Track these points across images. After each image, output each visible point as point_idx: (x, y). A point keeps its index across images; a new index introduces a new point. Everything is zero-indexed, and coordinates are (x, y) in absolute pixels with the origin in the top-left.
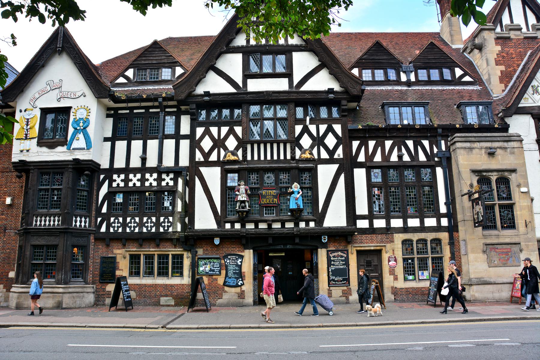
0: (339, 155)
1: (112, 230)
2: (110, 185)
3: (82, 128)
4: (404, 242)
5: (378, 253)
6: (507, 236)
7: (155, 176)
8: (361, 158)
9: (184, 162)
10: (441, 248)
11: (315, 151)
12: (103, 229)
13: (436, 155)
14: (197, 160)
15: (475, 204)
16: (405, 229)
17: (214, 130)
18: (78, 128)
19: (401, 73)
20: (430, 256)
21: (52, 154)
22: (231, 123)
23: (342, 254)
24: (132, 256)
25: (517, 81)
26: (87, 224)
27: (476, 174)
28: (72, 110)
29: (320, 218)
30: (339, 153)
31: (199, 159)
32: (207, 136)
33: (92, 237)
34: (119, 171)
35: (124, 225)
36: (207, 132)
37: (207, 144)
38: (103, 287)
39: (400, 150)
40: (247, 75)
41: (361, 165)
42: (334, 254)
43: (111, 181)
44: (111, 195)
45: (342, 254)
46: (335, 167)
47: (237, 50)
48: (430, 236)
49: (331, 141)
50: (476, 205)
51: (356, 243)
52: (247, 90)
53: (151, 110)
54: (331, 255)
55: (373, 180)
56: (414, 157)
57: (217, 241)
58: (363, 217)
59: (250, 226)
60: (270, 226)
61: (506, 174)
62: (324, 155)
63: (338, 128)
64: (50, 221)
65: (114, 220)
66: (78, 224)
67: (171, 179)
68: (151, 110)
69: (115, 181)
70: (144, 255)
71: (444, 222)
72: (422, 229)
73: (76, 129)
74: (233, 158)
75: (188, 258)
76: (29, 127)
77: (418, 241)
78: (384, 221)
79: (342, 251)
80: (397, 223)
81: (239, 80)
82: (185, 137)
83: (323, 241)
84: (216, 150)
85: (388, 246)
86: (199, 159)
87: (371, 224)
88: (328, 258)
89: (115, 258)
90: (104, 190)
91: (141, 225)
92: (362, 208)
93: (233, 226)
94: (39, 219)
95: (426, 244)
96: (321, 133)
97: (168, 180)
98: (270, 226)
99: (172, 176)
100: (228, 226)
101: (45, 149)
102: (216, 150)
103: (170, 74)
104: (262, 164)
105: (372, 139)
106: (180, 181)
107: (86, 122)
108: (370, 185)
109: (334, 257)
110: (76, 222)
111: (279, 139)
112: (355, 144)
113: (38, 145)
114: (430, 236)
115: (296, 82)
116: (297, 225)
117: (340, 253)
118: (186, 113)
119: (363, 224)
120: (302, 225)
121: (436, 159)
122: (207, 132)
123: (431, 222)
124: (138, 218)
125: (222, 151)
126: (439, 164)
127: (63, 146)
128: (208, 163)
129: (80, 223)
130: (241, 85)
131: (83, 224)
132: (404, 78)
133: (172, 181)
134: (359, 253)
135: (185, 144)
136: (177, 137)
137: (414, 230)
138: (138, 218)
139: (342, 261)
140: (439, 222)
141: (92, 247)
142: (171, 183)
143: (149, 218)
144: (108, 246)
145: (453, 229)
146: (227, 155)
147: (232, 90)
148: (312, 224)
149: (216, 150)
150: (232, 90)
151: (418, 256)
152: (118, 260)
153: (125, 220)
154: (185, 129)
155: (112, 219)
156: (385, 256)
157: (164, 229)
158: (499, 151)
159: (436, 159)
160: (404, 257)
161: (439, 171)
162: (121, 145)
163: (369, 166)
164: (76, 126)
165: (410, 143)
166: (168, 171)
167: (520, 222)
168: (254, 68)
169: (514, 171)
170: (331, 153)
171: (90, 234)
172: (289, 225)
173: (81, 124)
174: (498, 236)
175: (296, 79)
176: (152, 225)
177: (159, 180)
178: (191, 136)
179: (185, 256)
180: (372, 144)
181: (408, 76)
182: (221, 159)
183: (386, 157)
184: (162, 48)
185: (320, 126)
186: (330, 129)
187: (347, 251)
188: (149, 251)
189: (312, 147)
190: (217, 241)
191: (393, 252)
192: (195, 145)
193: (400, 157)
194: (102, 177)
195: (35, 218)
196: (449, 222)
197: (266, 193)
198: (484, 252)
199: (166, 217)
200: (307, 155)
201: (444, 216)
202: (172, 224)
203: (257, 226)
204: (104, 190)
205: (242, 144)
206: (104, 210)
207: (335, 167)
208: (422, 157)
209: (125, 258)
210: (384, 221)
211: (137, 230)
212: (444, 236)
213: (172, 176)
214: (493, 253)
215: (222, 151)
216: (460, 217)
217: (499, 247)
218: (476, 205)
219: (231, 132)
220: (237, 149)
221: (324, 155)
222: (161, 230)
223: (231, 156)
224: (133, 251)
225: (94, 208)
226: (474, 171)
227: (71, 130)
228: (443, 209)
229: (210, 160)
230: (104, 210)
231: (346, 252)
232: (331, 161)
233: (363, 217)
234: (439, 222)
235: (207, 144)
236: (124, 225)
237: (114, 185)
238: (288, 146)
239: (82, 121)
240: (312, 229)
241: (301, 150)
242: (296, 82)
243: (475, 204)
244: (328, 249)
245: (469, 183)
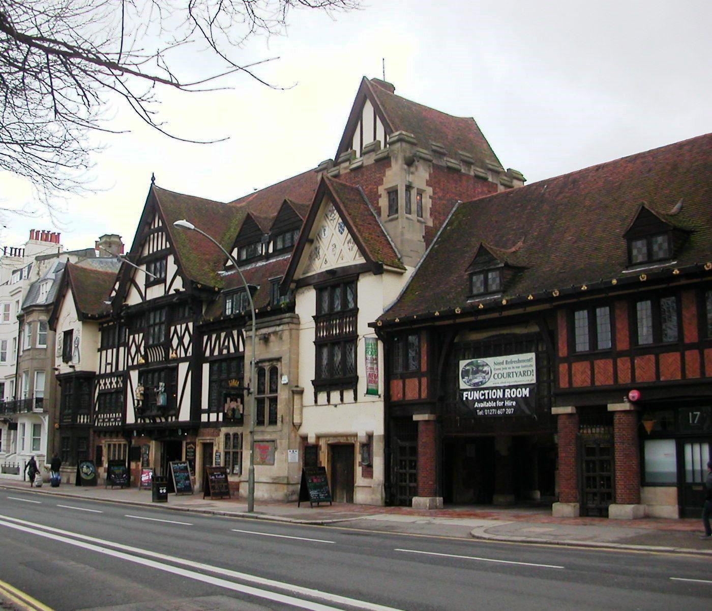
4: (227, 436)
25: (359, 227)
26: (89, 420)
33: (91, 432)
43: (100, 385)
58: (205, 411)
85: (217, 438)
110: (80, 419)
116: (167, 419)
128: (133, 368)
129: (83, 419)
131: (85, 420)
141: (91, 438)
156: (215, 449)
158: (272, 338)
187: (195, 443)
195: (79, 416)
217: (262, 444)
233: (205, 411)
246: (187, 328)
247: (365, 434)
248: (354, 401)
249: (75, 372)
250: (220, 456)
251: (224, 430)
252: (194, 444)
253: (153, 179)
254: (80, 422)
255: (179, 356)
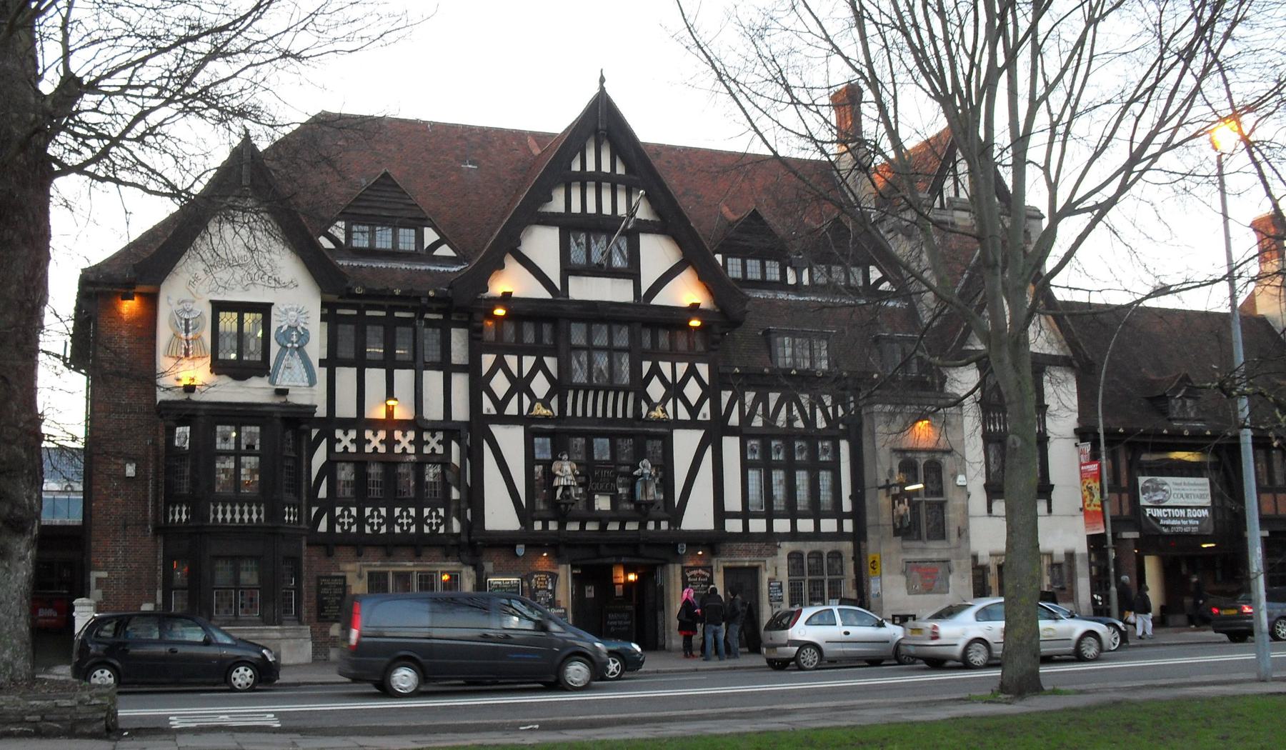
0: (705, 415)
1: (338, 529)
2: (331, 449)
3: (296, 345)
4: (791, 556)
5: (754, 571)
6: (935, 551)
7: (411, 435)
8: (734, 420)
9: (460, 412)
10: (841, 567)
11: (669, 406)
12: (323, 527)
13: (842, 420)
14: (485, 412)
15: (896, 502)
16: (794, 535)
17: (512, 361)
18: (289, 345)
19: (788, 269)
20: (827, 577)
21: (241, 390)
22: (538, 350)
23: (703, 573)
24: (371, 574)
27: (899, 455)
28: (274, 310)
29: (676, 514)
30: (705, 412)
31: (489, 410)
32: (500, 370)
34: (346, 424)
35: (361, 520)
36: (500, 364)
37: (500, 384)
38: (324, 630)
39: (789, 410)
40: (568, 270)
41: (732, 432)
42: (692, 573)
44: (329, 468)
45: (703, 573)
46: (697, 435)
47: (548, 220)
48: (827, 547)
49: (693, 391)
50: (899, 503)
51: (723, 555)
52: (568, 296)
53: (397, 314)
54: (688, 575)
55: (749, 457)
56: (810, 422)
57: (520, 550)
59: (573, 527)
60: (603, 527)
61: (938, 456)
62: (683, 414)
63: (703, 369)
64: (242, 513)
65: (343, 511)
66: (220, 517)
67: (439, 442)
68: (397, 314)
69: (340, 441)
70: (393, 573)
71: (848, 526)
72: (817, 535)
73: (284, 347)
74: (545, 412)
75: (469, 577)
76: (190, 336)
77: (811, 554)
78: (764, 521)
79: (703, 568)
80: (782, 525)
81: (555, 276)
82: (460, 369)
83: (680, 552)
84: (516, 396)
85: (769, 560)
86: (489, 410)
87: (746, 526)
88: (682, 579)
89: (344, 578)
90: (320, 457)
91: (390, 520)
92: (733, 502)
93: (545, 526)
94: (220, 508)
95: (822, 558)
96: (679, 378)
97: (433, 444)
98: (603, 527)
99: (440, 436)
100: (538, 526)
101: (225, 380)
102: (516, 397)
103: (413, 240)
104: (578, 425)
105: (749, 388)
106: (455, 446)
107: (304, 337)
108: (746, 466)
109: (692, 576)
111: (616, 382)
112: (726, 396)
113: (211, 372)
114: (827, 547)
115: (645, 287)
116: (643, 525)
117: (700, 571)
118: (459, 325)
119: (734, 526)
120: (651, 526)
121: (841, 427)
122: (500, 364)
123: (828, 525)
124: (385, 509)
125: (525, 396)
126: (845, 435)
127: (261, 375)
128: (503, 419)
130: (558, 285)
132: (791, 280)
133: (442, 447)
134: (726, 570)
135: (460, 383)
136: (447, 368)
137: (806, 537)
138: (385, 509)
139: (704, 583)
140: (840, 525)
142: (440, 450)
143: (405, 509)
144: (329, 554)
145: (858, 537)
146: (536, 407)
147: (545, 294)
148: (664, 525)
149: (516, 396)
150: (545, 294)
151: (810, 577)
152: (349, 582)
153: (361, 512)
154: (459, 353)
155: (338, 511)
156: (765, 577)
157: (430, 528)
159: (841, 427)
160: (792, 578)
161: (844, 446)
162: (346, 376)
163: (743, 432)
164: (285, 343)
165: (805, 399)
166: (433, 428)
167: (952, 529)
168: (577, 256)
169: (949, 452)
170: (694, 410)
171: (302, 535)
172: (632, 526)
173: (294, 339)
174: (923, 550)
175: (645, 285)
176: (381, 521)
177: (419, 443)
178: (472, 368)
179: (464, 575)
180: (750, 396)
181: (799, 277)
182: (525, 413)
183: (770, 419)
184: (397, 186)
185: (678, 365)
186: (692, 372)
187: (711, 567)
188: (405, 566)
189: (664, 400)
190: (520, 550)
191: (776, 571)
192: (479, 385)
193: (790, 420)
194: (314, 433)
196: (855, 525)
197: (600, 474)
198: (904, 573)
199: (434, 509)
200: (658, 413)
201: (848, 516)
202: (446, 521)
203: (583, 526)
204: (320, 457)
205: (559, 387)
206: (322, 493)
207: (697, 435)
208: (821, 424)
209: (360, 576)
210: (764, 521)
211: (384, 530)
212: (847, 547)
213: (440, 436)
214: (915, 573)
215: (525, 397)
216: (870, 519)
217: (923, 565)
218: (899, 503)
219: (539, 366)
220: (549, 395)
221: (683, 414)
222: (426, 530)
223: (541, 408)
224: (375, 566)
225: (304, 490)
226: (894, 450)
227: (275, 348)
228: (847, 506)
229: (507, 412)
230: (322, 493)
231: (709, 570)
232: (692, 424)
234: (840, 525)
235: (500, 384)
236: (361, 520)
237: (339, 448)
238: (631, 396)
239: (294, 333)
240: (664, 532)
241: (648, 405)
242: (645, 287)
243: (896, 502)
244: (684, 565)
245: (887, 469)
246: (692, 372)
247: (1063, 553)
248: (1046, 514)
249: (287, 405)
250: (780, 587)
251: (787, 547)
252: (709, 569)
253: (602, 80)
254: (216, 519)
255: (671, 417)
